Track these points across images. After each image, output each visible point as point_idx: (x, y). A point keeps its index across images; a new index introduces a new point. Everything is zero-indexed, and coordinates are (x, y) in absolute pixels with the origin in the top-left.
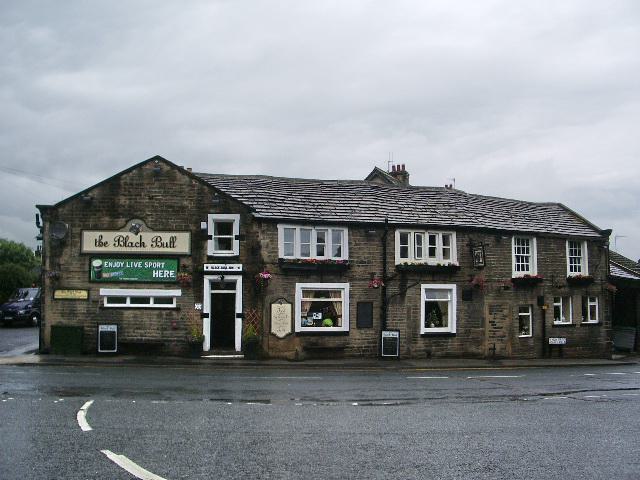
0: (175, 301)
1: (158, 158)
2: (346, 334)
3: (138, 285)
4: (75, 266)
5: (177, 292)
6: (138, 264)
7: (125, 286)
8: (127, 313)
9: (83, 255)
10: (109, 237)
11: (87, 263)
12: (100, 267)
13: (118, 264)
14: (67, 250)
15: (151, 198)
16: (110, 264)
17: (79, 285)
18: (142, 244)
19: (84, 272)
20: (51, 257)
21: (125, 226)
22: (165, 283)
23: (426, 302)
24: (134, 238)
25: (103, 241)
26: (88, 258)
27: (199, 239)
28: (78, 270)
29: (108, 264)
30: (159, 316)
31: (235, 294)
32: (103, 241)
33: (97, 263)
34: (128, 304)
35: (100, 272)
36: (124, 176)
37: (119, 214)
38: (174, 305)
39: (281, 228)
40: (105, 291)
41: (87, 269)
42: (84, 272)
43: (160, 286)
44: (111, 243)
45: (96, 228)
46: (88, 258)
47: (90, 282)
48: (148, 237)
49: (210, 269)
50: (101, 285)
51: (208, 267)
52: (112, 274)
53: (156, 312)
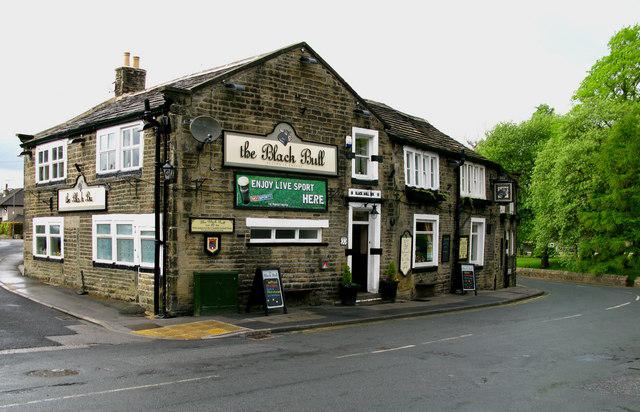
0: (319, 234)
1: (304, 45)
2: (435, 269)
3: (288, 214)
4: (215, 184)
5: (324, 223)
6: (286, 185)
7: (273, 213)
8: (276, 251)
9: (225, 168)
10: (257, 144)
11: (231, 180)
12: (247, 186)
13: (267, 183)
14: (205, 160)
15: (298, 97)
16: (258, 184)
17: (221, 212)
18: (292, 159)
19: (227, 193)
20: (184, 170)
21: (273, 131)
22: (314, 211)
23: (354, 226)
24: (283, 150)
25: (250, 149)
26: (231, 173)
27: (344, 155)
28: (220, 190)
29: (257, 183)
30: (309, 253)
31: (367, 226)
32: (250, 149)
33: (242, 181)
34: (273, 239)
35: (247, 192)
36: (271, 62)
37: (162, 92)
38: (319, 240)
39: (406, 149)
40: (253, 222)
41: (230, 188)
42: (227, 193)
43: (308, 215)
44: (259, 153)
45: (239, 130)
46: (231, 173)
47: (236, 207)
48: (298, 148)
49: (354, 195)
50: (247, 213)
51: (353, 192)
52: (261, 198)
53: (305, 249)
